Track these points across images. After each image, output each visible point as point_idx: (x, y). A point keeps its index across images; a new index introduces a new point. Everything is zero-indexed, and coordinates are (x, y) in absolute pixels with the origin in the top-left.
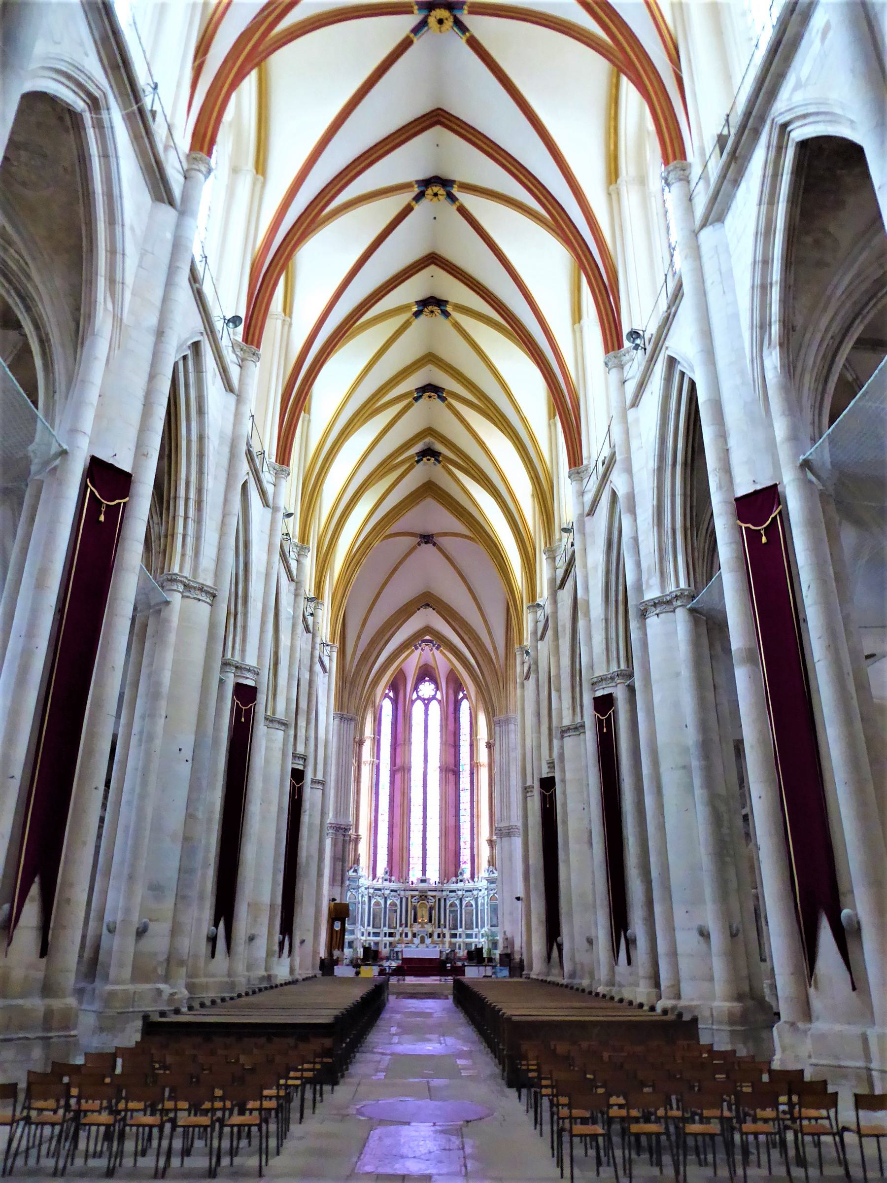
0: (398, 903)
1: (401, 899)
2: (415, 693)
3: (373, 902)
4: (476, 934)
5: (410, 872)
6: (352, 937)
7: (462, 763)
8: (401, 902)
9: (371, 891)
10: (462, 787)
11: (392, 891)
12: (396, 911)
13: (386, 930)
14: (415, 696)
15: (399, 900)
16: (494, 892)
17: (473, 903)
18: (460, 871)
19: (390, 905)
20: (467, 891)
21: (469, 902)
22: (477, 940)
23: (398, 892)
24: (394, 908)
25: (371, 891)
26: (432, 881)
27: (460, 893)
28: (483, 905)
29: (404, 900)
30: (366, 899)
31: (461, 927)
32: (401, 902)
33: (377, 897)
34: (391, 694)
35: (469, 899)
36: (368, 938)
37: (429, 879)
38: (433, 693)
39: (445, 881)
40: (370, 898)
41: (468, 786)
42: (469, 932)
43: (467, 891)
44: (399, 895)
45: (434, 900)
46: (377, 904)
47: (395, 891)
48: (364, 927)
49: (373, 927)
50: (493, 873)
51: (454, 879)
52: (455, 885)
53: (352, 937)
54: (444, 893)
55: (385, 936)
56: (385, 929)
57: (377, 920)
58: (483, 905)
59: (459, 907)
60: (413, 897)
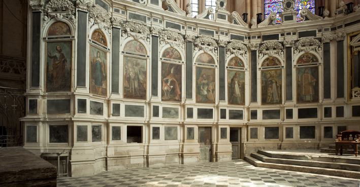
0: (319, 55)
1: (326, 47)
8: (326, 53)
9: (256, 42)
11: (302, 35)
12: (316, 69)
15: (321, 51)
19: (300, 60)
23: (319, 35)
24: (311, 65)
25: (256, 42)
29: (333, 49)
32: (326, 53)
40: (254, 54)
44: (320, 40)
46: (272, 61)
47: (313, 33)
49: (264, 101)
57: (273, 90)
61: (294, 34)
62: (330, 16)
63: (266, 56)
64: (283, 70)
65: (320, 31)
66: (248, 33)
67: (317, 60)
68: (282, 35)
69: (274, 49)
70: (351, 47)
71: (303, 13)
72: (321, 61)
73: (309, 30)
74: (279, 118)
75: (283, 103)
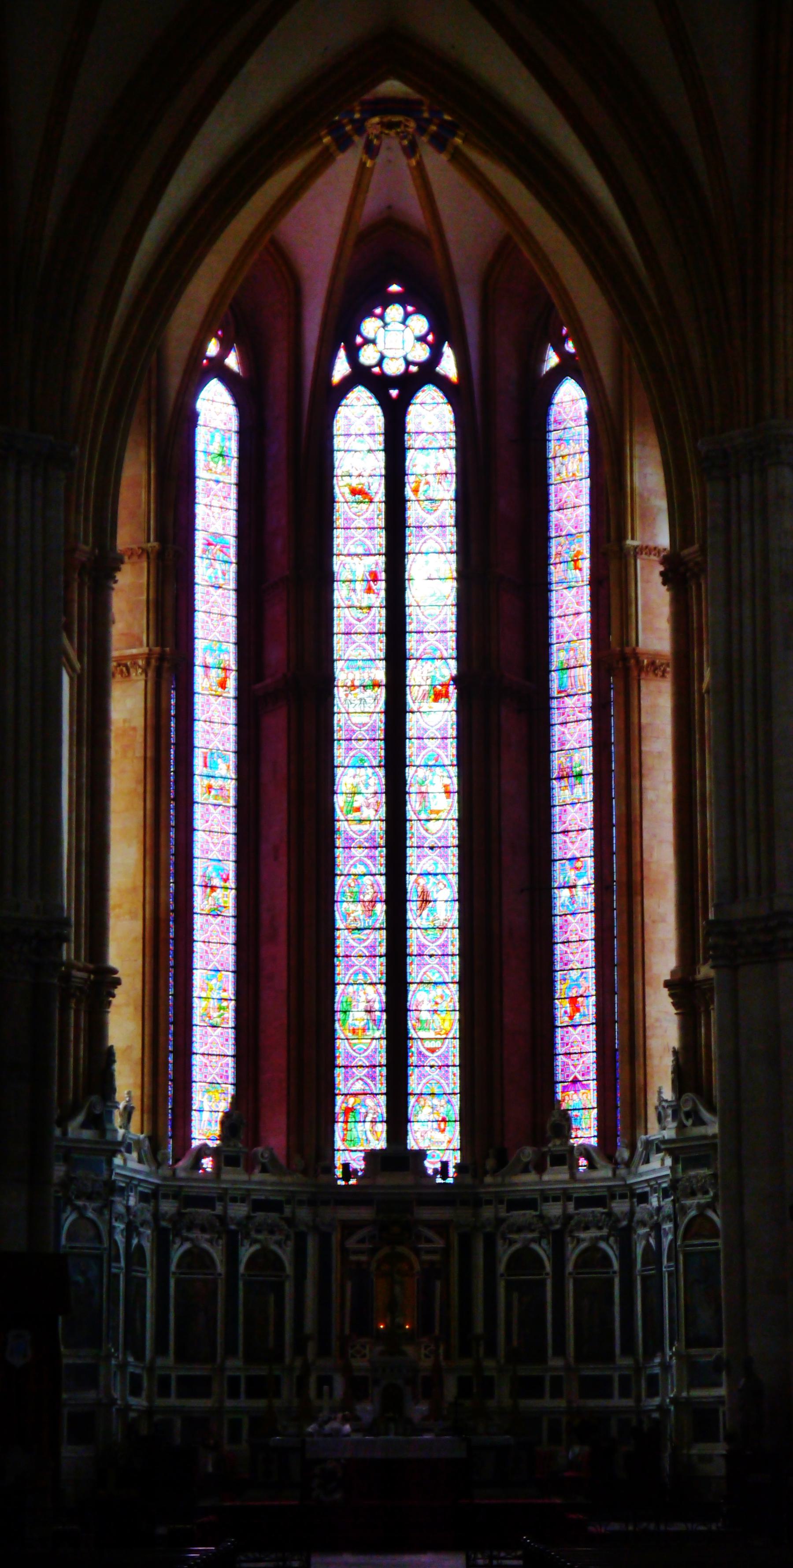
0: (286, 1255)
2: (342, 353)
3: (178, 1252)
4: (625, 1381)
5: (339, 1128)
6: (91, 1395)
7: (558, 657)
9: (168, 1207)
10: (557, 760)
11: (258, 1205)
12: (278, 1289)
13: (235, 1365)
14: (341, 368)
15: (290, 1244)
16: (701, 1199)
17: (610, 1250)
18: (555, 1118)
20: (582, 1202)
21: (594, 1248)
22: (629, 1402)
23: (288, 1210)
25: (168, 1207)
26: (431, 1165)
27: (554, 1210)
28: (653, 1256)
29: (311, 1245)
30: (146, 1240)
31: (560, 1350)
33: (195, 1234)
34: (232, 361)
35: (593, 1233)
36: (160, 1402)
37: (421, 1154)
38: (422, 353)
39: (490, 1163)
41: (584, 760)
42: (591, 1370)
43: (582, 1202)
45: (439, 1243)
48: (140, 1356)
49: (181, 1356)
50: (700, 1122)
51: (528, 1153)
52: (532, 1177)
53: (91, 1395)
54: (487, 1213)
55: (234, 1393)
56: (230, 1363)
58: (653, 1256)
59: (548, 1267)
60: (349, 1228)
61: (243, 1200)
62: (304, 1172)
63: (187, 1245)
64: (219, 1281)
65: (288, 1202)
66: (158, 1185)
67: (283, 1268)
68: (221, 1198)
69: (203, 1230)
70: (344, 1251)
71: (262, 1156)
72: (289, 1269)
73: (272, 1198)
74: (207, 1395)
75: (219, 1359)
